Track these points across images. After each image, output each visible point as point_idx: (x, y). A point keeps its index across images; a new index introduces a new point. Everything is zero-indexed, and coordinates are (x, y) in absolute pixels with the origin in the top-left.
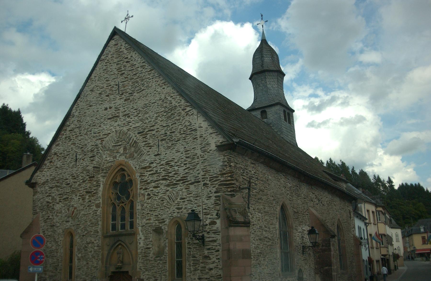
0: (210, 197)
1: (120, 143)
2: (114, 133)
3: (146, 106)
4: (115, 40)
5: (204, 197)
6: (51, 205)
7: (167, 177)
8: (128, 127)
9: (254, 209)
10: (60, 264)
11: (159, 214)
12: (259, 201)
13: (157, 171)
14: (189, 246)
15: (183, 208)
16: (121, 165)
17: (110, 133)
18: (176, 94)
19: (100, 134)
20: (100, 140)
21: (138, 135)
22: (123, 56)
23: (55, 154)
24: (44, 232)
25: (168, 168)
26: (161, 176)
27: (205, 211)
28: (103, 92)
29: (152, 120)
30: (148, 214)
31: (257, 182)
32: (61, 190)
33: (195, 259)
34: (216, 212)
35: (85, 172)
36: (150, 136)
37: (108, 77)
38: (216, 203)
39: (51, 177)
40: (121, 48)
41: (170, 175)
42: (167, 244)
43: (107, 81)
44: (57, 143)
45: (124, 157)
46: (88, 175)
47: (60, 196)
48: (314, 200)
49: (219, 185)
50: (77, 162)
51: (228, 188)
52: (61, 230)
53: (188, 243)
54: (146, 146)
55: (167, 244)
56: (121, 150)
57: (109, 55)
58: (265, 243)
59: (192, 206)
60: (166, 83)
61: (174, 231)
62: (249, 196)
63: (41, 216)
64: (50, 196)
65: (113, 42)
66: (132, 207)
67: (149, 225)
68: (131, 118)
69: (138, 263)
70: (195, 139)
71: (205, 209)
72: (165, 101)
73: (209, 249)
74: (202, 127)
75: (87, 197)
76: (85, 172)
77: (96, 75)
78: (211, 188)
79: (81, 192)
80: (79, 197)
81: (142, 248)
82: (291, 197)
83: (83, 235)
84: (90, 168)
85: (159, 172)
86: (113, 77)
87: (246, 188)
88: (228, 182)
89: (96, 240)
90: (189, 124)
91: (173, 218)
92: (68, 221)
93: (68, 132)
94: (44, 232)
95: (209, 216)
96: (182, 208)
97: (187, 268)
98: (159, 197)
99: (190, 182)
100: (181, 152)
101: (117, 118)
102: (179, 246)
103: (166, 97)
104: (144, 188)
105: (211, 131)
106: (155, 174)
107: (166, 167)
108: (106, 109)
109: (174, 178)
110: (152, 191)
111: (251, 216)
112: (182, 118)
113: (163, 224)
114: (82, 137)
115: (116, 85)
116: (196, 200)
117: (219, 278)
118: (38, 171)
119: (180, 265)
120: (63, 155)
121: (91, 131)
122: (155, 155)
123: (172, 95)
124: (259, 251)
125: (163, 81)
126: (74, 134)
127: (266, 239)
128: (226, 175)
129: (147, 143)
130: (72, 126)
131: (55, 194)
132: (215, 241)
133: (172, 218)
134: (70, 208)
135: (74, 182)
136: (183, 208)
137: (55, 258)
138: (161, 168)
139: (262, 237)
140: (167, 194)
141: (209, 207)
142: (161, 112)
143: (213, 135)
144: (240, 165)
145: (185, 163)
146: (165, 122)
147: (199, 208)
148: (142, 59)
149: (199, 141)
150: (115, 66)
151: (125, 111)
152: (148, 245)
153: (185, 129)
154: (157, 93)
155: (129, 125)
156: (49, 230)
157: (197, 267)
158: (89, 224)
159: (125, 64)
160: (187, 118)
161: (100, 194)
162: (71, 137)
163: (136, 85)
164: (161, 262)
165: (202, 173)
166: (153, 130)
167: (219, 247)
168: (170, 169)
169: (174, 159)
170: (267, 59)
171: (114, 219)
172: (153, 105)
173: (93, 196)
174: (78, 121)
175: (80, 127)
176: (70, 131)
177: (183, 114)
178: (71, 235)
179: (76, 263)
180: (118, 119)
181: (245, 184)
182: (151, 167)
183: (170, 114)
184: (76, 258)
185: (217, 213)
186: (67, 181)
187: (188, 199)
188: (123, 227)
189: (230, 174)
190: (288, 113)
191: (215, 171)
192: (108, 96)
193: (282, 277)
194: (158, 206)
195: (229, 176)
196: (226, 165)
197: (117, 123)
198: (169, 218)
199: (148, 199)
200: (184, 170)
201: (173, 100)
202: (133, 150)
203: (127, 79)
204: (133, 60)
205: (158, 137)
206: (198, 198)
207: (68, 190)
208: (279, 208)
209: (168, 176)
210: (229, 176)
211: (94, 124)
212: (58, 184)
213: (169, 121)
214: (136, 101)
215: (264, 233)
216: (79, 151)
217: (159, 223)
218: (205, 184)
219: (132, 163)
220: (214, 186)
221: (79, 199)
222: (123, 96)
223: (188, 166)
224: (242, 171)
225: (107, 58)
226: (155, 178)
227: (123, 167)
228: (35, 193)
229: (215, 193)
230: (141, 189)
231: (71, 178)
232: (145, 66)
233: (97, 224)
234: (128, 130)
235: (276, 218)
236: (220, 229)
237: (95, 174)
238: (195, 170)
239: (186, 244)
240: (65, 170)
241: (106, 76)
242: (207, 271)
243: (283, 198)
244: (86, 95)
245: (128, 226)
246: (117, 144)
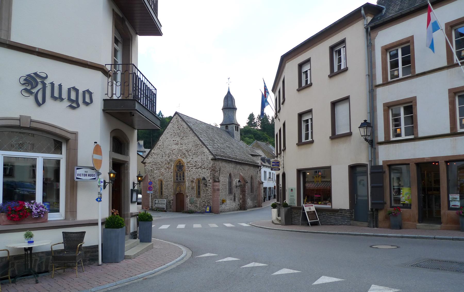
66: (184, 173)
84: (168, 160)
102: (199, 187)
119: (199, 192)
130: (160, 144)
170: (229, 102)
171: (177, 177)
178: (161, 181)
188: (180, 179)
216: (163, 153)
219: (183, 160)
226: (191, 166)
228: (145, 166)
233: (171, 178)
245: (182, 179)
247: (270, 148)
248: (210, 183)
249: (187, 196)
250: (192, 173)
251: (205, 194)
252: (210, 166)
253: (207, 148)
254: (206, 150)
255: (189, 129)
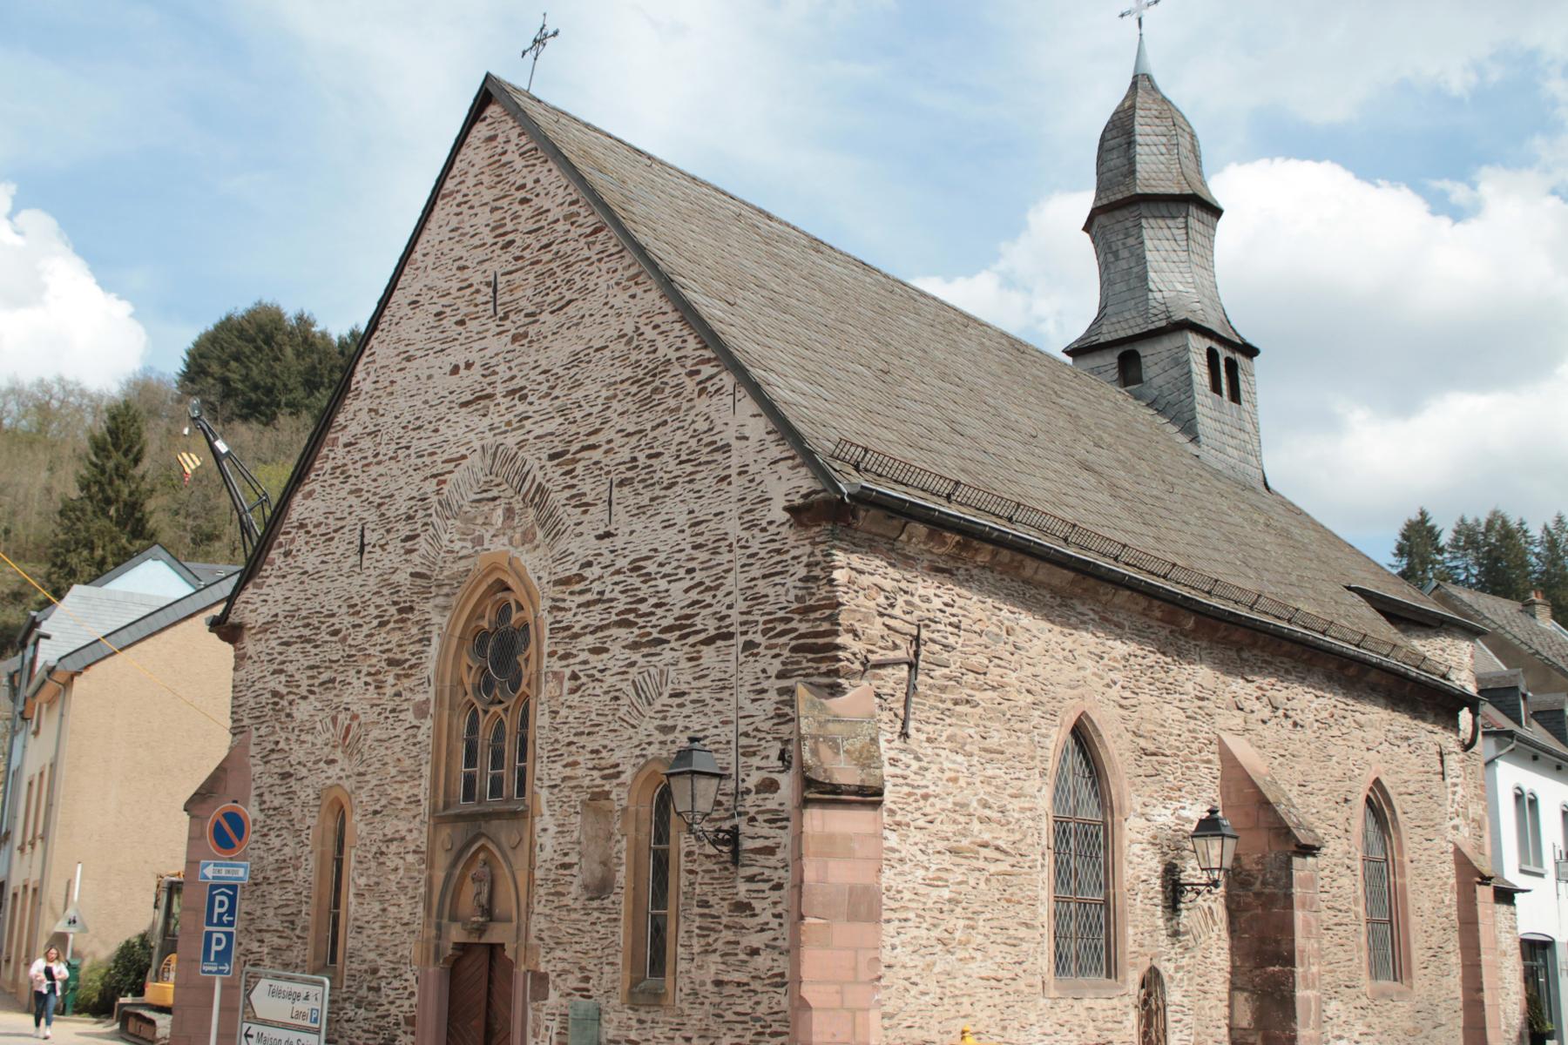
0: (764, 691)
1: (494, 493)
2: (474, 460)
3: (576, 360)
4: (489, 121)
5: (745, 689)
6: (285, 703)
7: (631, 617)
8: (518, 436)
9: (929, 740)
10: (304, 908)
11: (605, 747)
12: (958, 708)
13: (602, 593)
14: (690, 866)
15: (680, 728)
16: (494, 568)
17: (464, 457)
18: (676, 316)
19: (435, 458)
20: (435, 481)
21: (549, 464)
22: (512, 178)
23: (302, 526)
24: (261, 795)
25: (636, 581)
26: (614, 611)
27: (744, 741)
28: (448, 310)
29: (595, 410)
30: (570, 744)
31: (951, 640)
32: (314, 651)
33: (706, 911)
34: (779, 745)
35: (385, 592)
36: (587, 468)
37: (465, 255)
38: (779, 716)
39: (288, 607)
40: (505, 153)
41: (644, 608)
42: (624, 856)
43: (461, 268)
44: (307, 488)
45: (505, 540)
46: (395, 603)
47: (310, 673)
48: (1247, 705)
49: (794, 650)
50: (366, 555)
51: (821, 660)
52: (310, 791)
53: (689, 854)
54: (573, 502)
55: (624, 856)
56: (498, 517)
57: (470, 175)
58: (981, 864)
59: (705, 720)
60: (640, 280)
61: (647, 810)
62: (912, 689)
63: (254, 740)
64: (281, 671)
65: (481, 131)
67: (573, 783)
68: (531, 404)
69: (534, 917)
70: (723, 479)
71: (746, 735)
72: (635, 343)
73: (751, 879)
74: (747, 438)
75: (391, 680)
76: (385, 592)
77: (429, 249)
78: (768, 659)
79: (374, 661)
80: (369, 679)
81: (548, 865)
82: (1127, 694)
83: (376, 812)
84: (402, 577)
85: (607, 596)
86: (480, 254)
87: (896, 663)
88: (820, 641)
89: (410, 831)
90: (706, 426)
91: (647, 763)
92: (333, 761)
93: (340, 451)
94: (261, 795)
95: (756, 761)
96: (674, 727)
97: (680, 941)
98: (605, 686)
99: (703, 636)
100: (677, 528)
101: (486, 402)
102: (662, 864)
103: (637, 328)
104: (561, 652)
105: (775, 451)
106: (596, 602)
107: (630, 581)
108: (455, 370)
109: (654, 619)
110: (585, 662)
111: (915, 765)
112: (685, 406)
113: (615, 782)
114: (381, 469)
115: (488, 284)
116: (719, 700)
117: (777, 985)
118: (250, 586)
119: (659, 931)
120: (323, 529)
121: (408, 448)
122: (599, 537)
123: (658, 320)
124: (946, 893)
125: (633, 270)
126: (357, 457)
127: (984, 852)
128: (817, 615)
129: (574, 491)
130: (354, 428)
131: (298, 665)
132: (770, 851)
133: (642, 761)
134: (340, 717)
135: (354, 626)
136: (680, 728)
137: (290, 887)
138: (616, 583)
139: (965, 842)
140: (630, 677)
141: (757, 729)
142: (622, 382)
143: (782, 467)
144: (877, 579)
145: (690, 565)
146: (634, 418)
147: (727, 728)
148: (570, 190)
149: (735, 490)
150: (485, 216)
151: (513, 378)
152: (566, 854)
153: (693, 442)
154: (611, 312)
155: (522, 427)
156: (277, 790)
157: (710, 940)
158: (393, 772)
159: (516, 207)
160: (702, 404)
161: (430, 667)
162: (350, 466)
163: (549, 282)
164: (604, 917)
165: (742, 606)
166: (593, 447)
167: (781, 873)
168: (644, 587)
169: (655, 550)
171: (471, 760)
172: (599, 355)
173: (407, 676)
174: (370, 410)
175: (374, 434)
176: (346, 445)
177: (689, 389)
179: (352, 909)
180: (492, 408)
181: (896, 647)
182: (584, 579)
183: (649, 388)
184: (352, 890)
185: (783, 752)
186: (332, 620)
187: (694, 696)
188: (496, 789)
189: (828, 612)
190: (1228, 360)
191: (782, 599)
192: (461, 323)
193: (1053, 993)
194: (602, 719)
195: (824, 619)
196: (816, 578)
197: (487, 421)
198: (633, 761)
199: (573, 691)
200: (686, 591)
201: (660, 338)
202: (531, 518)
203: (520, 264)
204: (543, 194)
205: (608, 473)
206: (725, 694)
207: (335, 651)
208: (1058, 736)
209: (634, 611)
210: (824, 619)
211: (419, 423)
212: (307, 632)
213: (646, 415)
214: (545, 343)
215: (976, 826)
216: (371, 516)
217: (604, 777)
218: (749, 645)
220: (777, 651)
221: (366, 684)
222: (508, 324)
223: (698, 576)
224: (881, 600)
225: (463, 188)
226: (595, 617)
227: (505, 578)
229: (778, 677)
230: (552, 654)
231: (344, 609)
232: (578, 214)
234: (521, 445)
235: (1042, 774)
236: (789, 806)
237: (415, 598)
238: (720, 594)
239: (683, 858)
240: (327, 584)
241: (459, 251)
242: (742, 957)
243: (1082, 697)
244: (395, 320)
246: (485, 495)
247: (1543, 632)
248: (776, 819)
249: (541, 980)
250: (594, 701)
251: (714, 966)
252: (782, 594)
253: (756, 391)
254: (745, 420)
255: (589, 220)
